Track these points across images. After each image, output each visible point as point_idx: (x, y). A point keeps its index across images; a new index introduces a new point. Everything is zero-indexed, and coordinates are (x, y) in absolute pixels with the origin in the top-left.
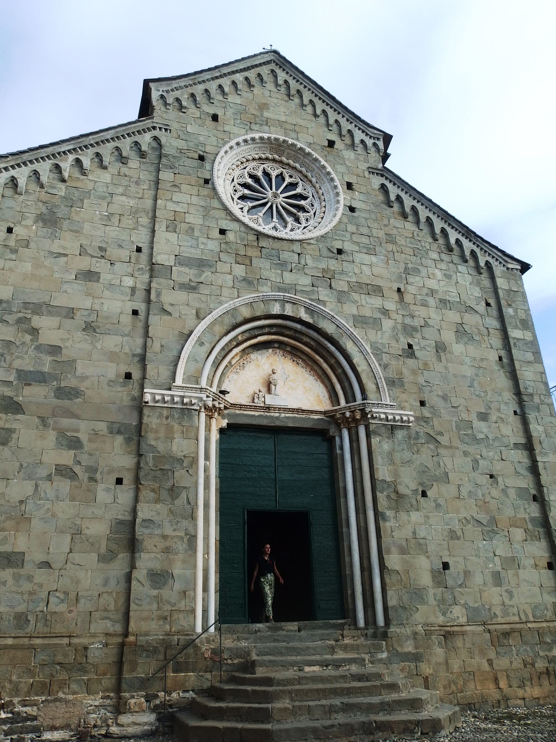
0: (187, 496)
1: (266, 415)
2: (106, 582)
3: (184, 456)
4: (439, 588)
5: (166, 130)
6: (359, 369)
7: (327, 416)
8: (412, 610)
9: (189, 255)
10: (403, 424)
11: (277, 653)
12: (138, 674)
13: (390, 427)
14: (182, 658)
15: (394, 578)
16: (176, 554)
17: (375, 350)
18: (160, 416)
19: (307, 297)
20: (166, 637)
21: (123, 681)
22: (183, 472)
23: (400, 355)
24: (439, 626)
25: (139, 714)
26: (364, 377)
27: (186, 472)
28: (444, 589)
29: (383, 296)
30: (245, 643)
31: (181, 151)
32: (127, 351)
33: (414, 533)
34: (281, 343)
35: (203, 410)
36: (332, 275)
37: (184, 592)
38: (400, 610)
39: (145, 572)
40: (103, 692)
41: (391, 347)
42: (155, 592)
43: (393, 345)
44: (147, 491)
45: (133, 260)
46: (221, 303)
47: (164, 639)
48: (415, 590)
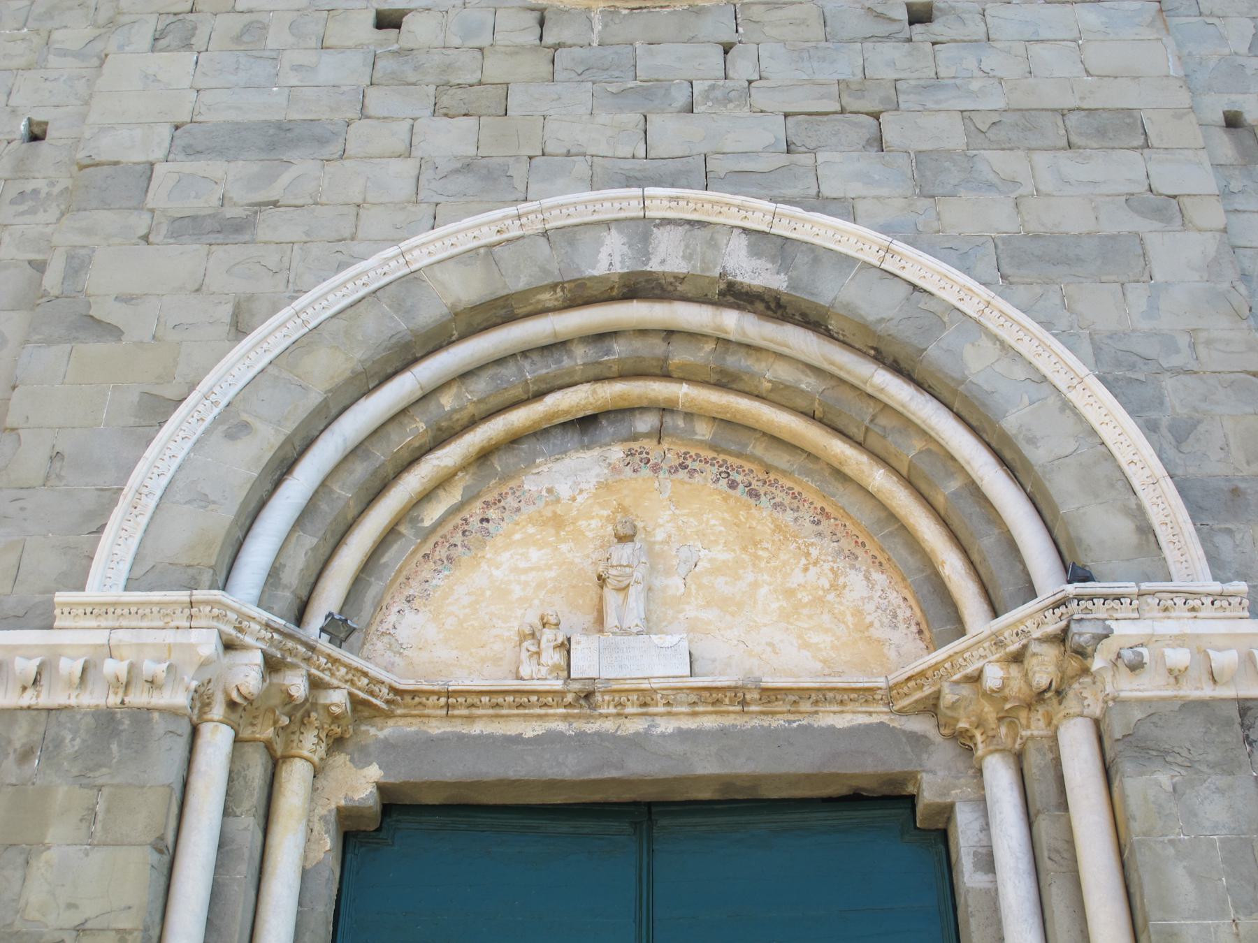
1: (581, 735)
6: (1038, 455)
7: (901, 712)
17: (1118, 364)
19: (763, 192)
29: (1147, 145)
34: (665, 409)
35: (218, 711)
41: (1209, 343)
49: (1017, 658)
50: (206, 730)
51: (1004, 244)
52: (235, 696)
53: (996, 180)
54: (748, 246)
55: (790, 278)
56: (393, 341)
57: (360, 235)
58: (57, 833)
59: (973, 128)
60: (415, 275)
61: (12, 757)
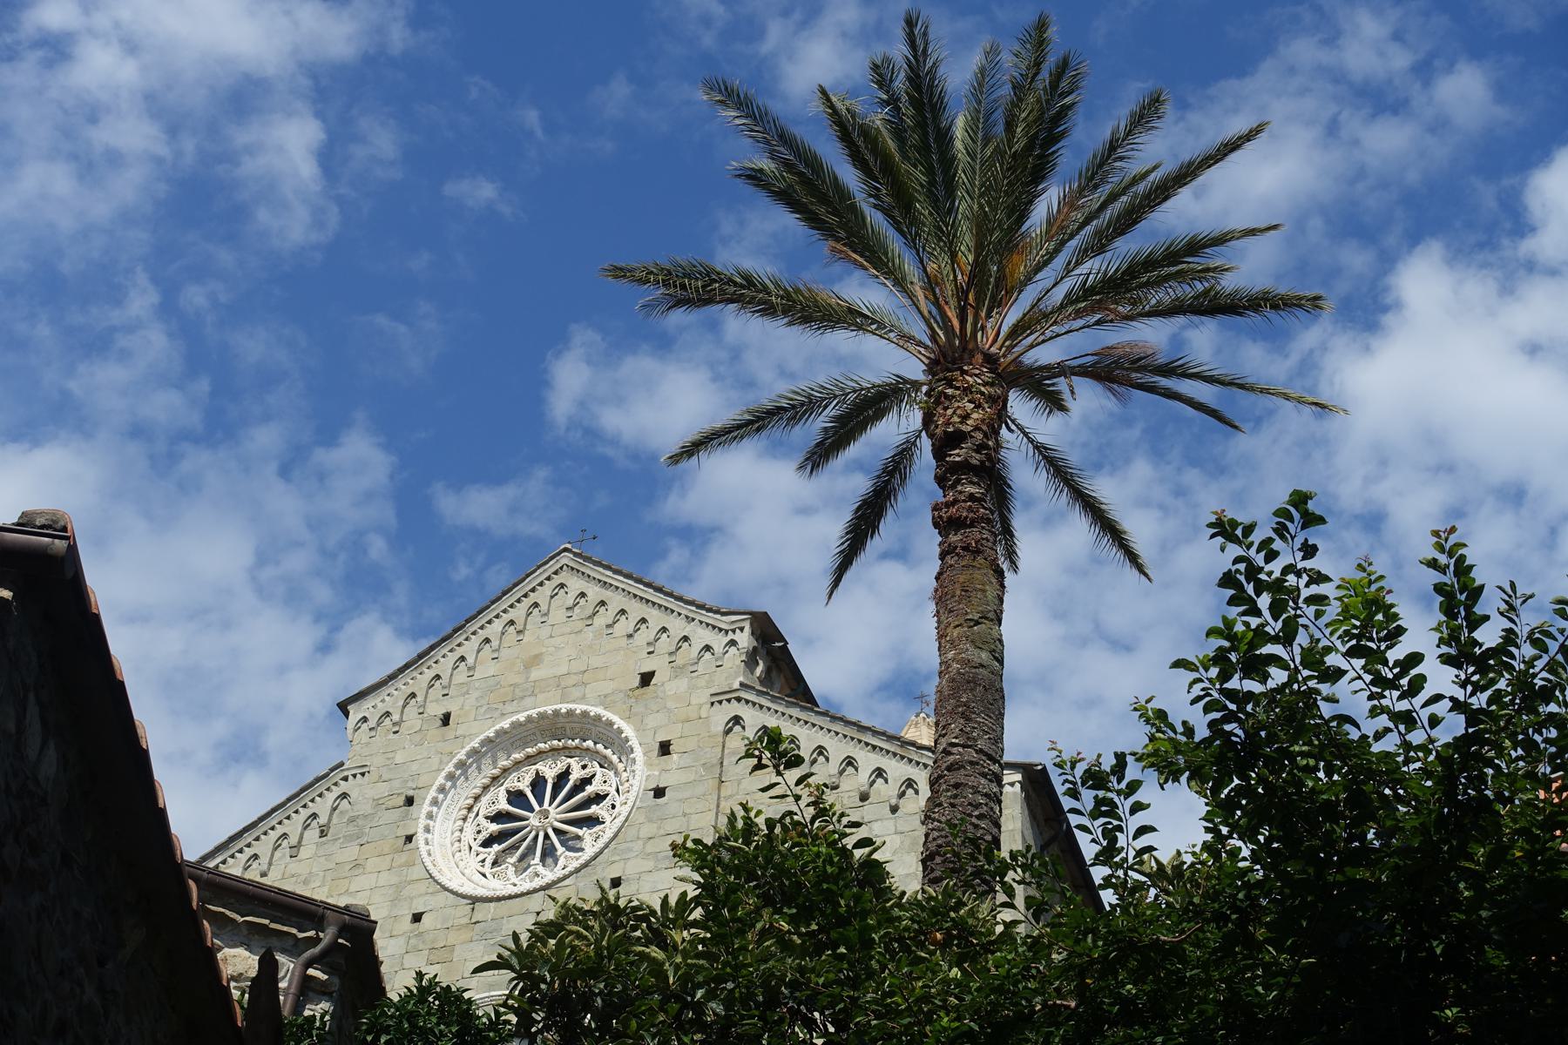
5: (363, 774)
31: (377, 803)
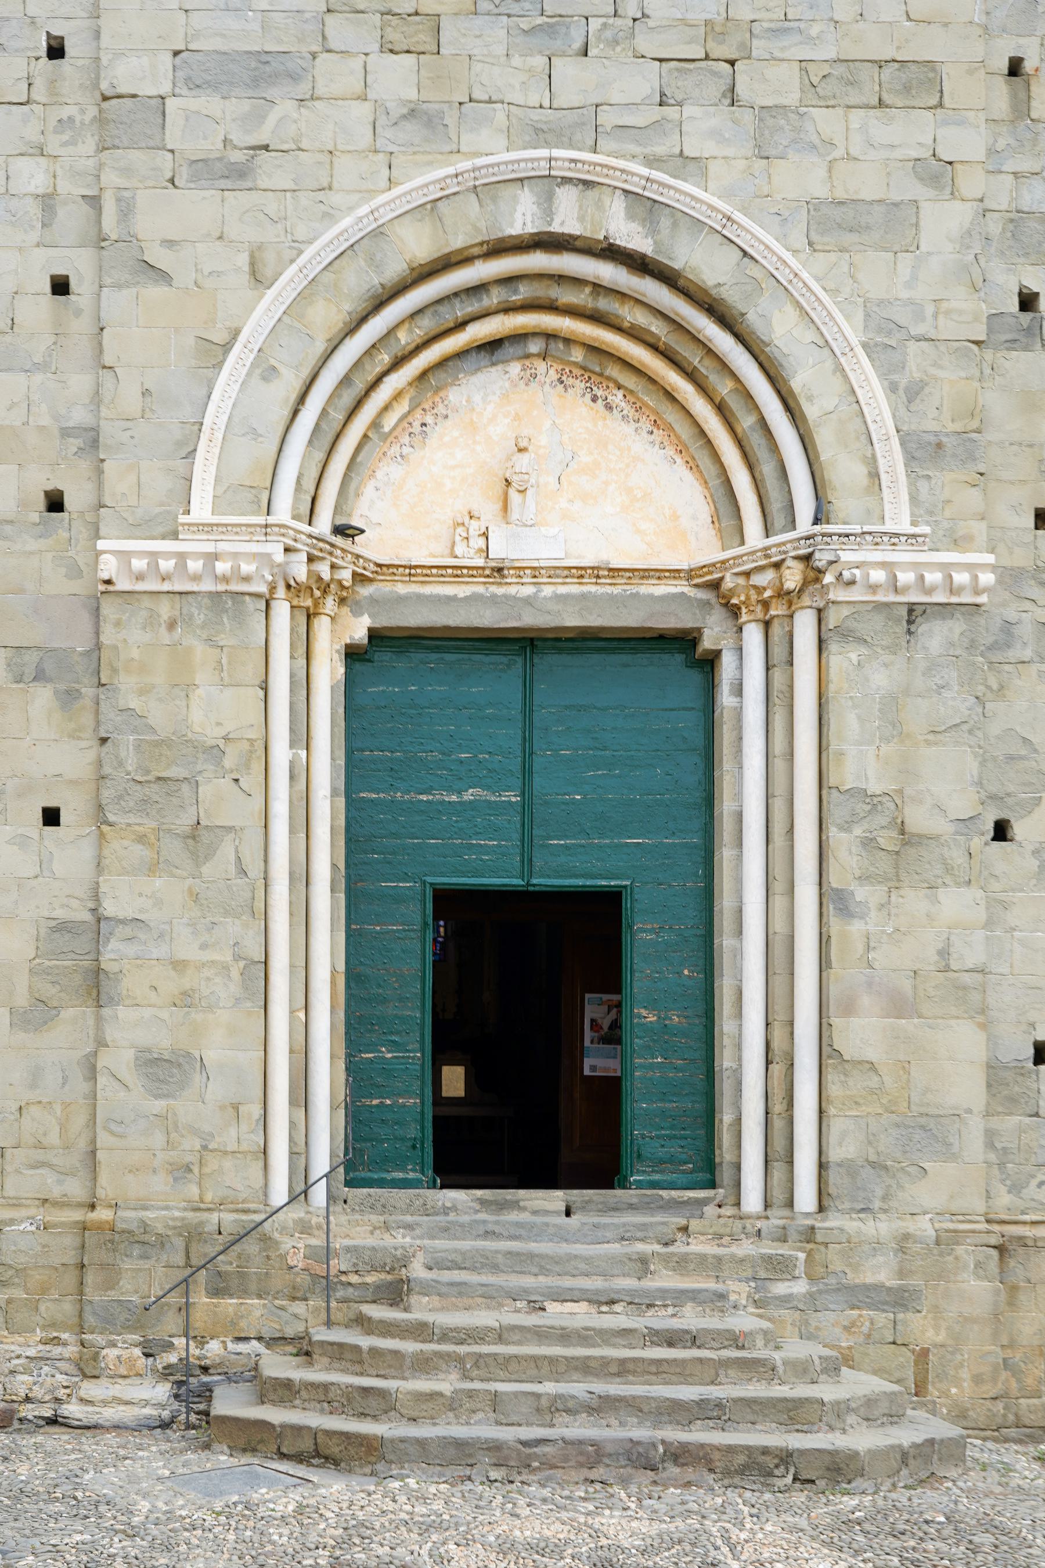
0: (237, 852)
2: (35, 1080)
3: (226, 738)
4: (1010, 1114)
6: (811, 411)
8: (909, 1174)
9: (218, 44)
10: (954, 600)
11: (484, 1265)
12: (122, 1293)
13: (904, 612)
14: (231, 1263)
15: (858, 1083)
16: (210, 1008)
17: (880, 330)
18: (151, 622)
20: (190, 1215)
21: (88, 1308)
22: (226, 783)
23: (977, 343)
24: (988, 1221)
25: (128, 1381)
26: (824, 439)
27: (233, 783)
28: (1028, 1120)
29: (941, 105)
30: (404, 1237)
32: (46, 421)
33: (944, 953)
35: (281, 592)
36: (742, 46)
37: (236, 1107)
38: (867, 1172)
39: (130, 1054)
40: (44, 1328)
41: (948, 313)
42: (159, 1105)
43: (954, 304)
44: (126, 843)
45: (39, 93)
46: (329, 217)
47: (183, 1219)
48: (923, 1121)
49: (777, 566)
50: (273, 603)
51: (815, 210)
52: (292, 583)
53: (817, 141)
54: (626, 208)
55: (655, 243)
56: (370, 294)
57: (335, 185)
58: (203, 677)
59: (807, 81)
60: (381, 229)
61: (163, 625)
